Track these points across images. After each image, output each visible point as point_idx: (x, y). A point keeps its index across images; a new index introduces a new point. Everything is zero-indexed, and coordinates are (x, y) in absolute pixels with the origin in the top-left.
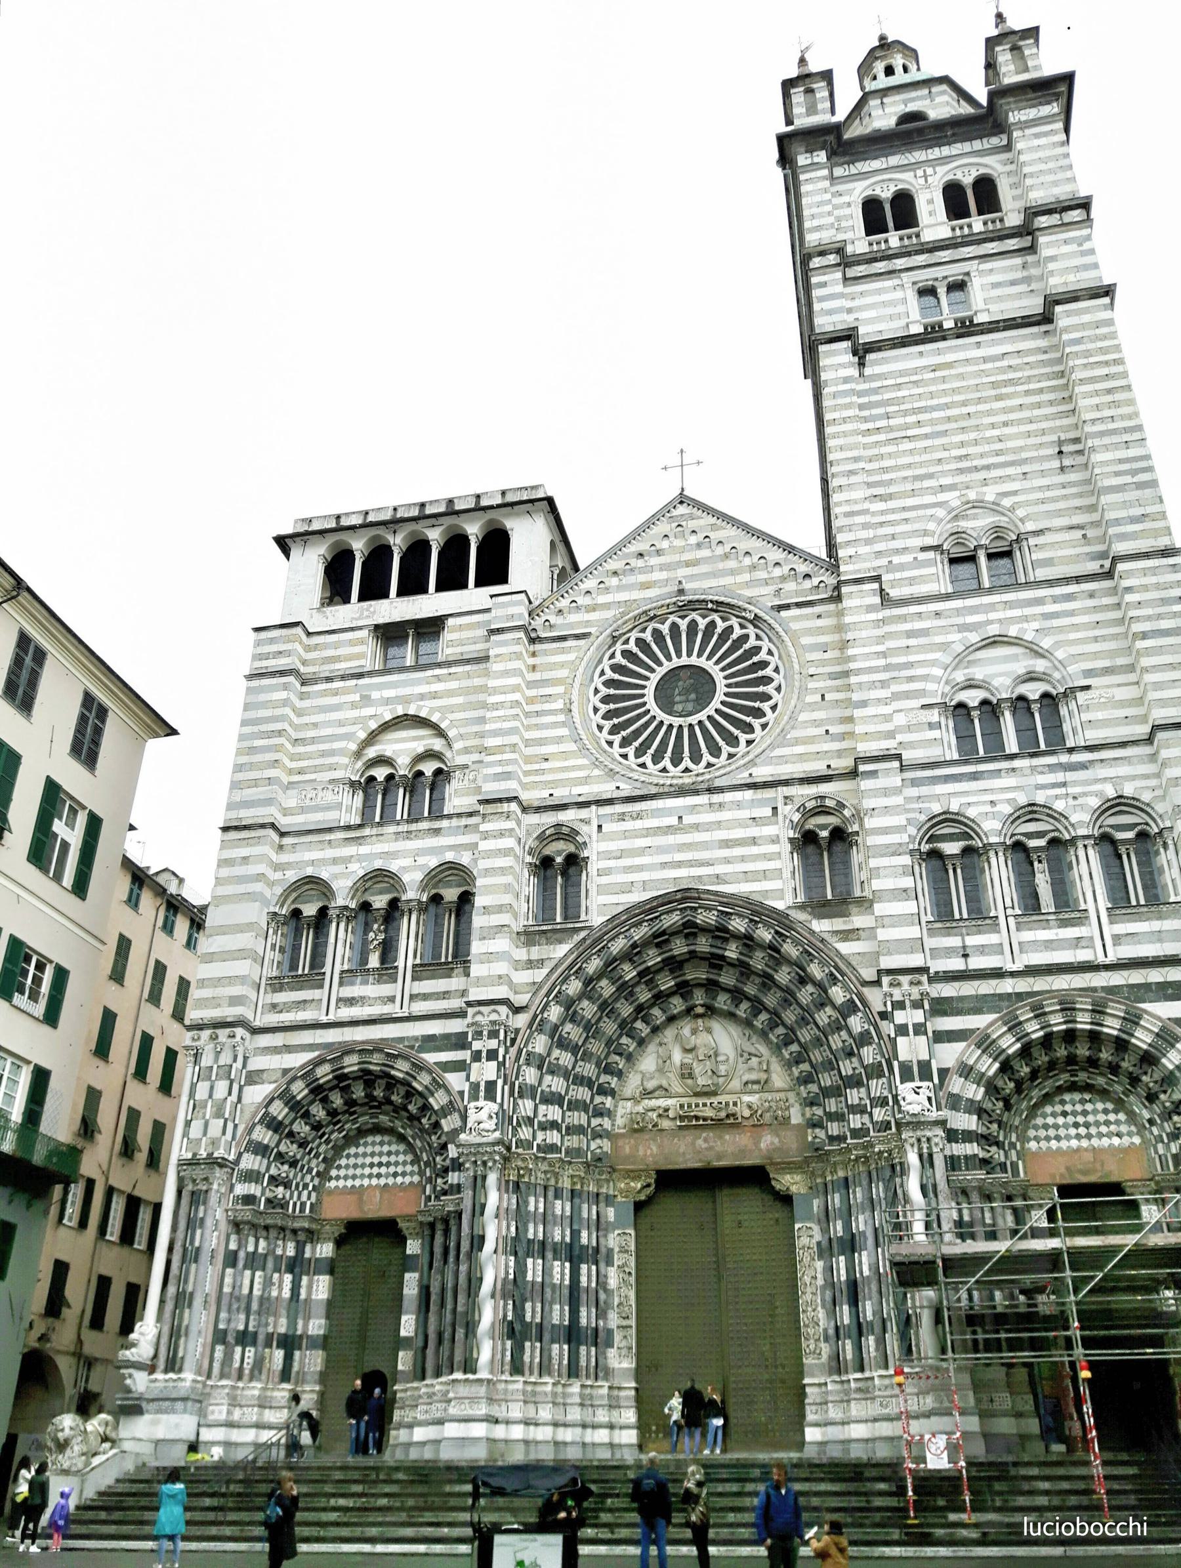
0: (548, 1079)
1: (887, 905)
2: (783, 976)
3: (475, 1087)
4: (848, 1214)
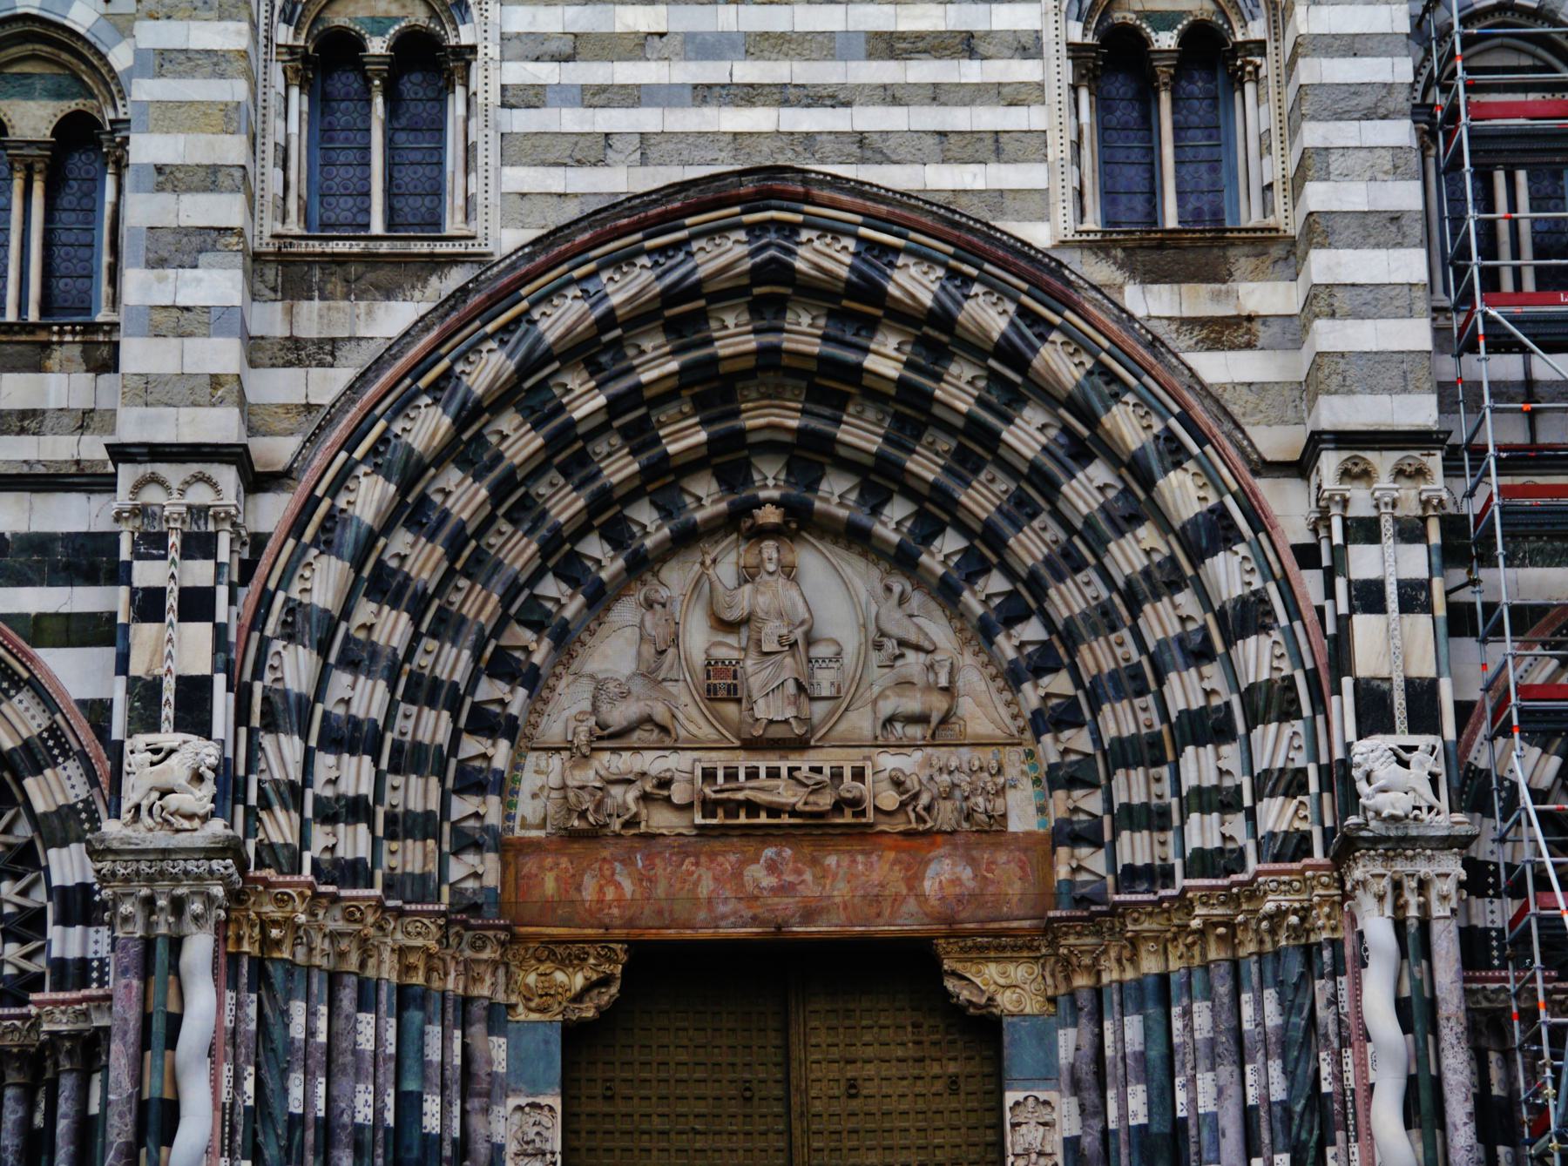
0: (341, 681)
1: (1346, 255)
2: (1028, 434)
3: (145, 694)
4: (1161, 1071)
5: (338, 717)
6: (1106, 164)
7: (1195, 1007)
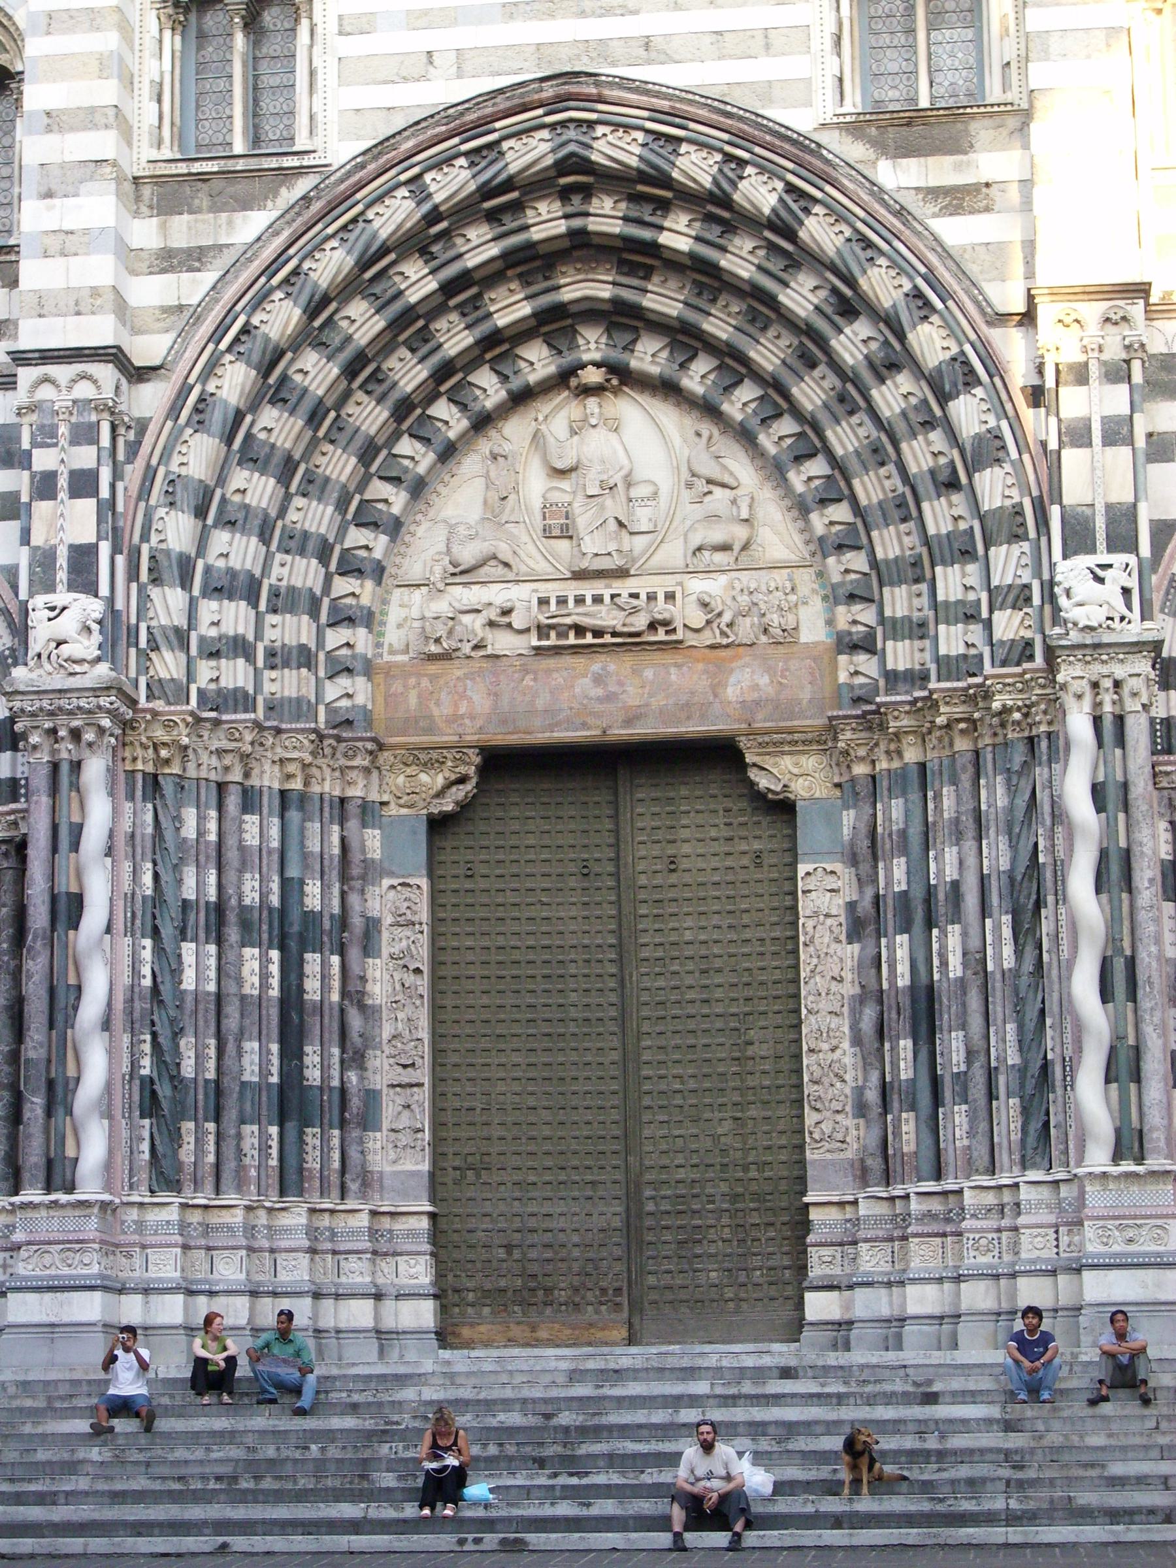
0: (221, 539)
3: (44, 560)
5: (219, 569)
6: (869, 53)
7: (945, 790)
